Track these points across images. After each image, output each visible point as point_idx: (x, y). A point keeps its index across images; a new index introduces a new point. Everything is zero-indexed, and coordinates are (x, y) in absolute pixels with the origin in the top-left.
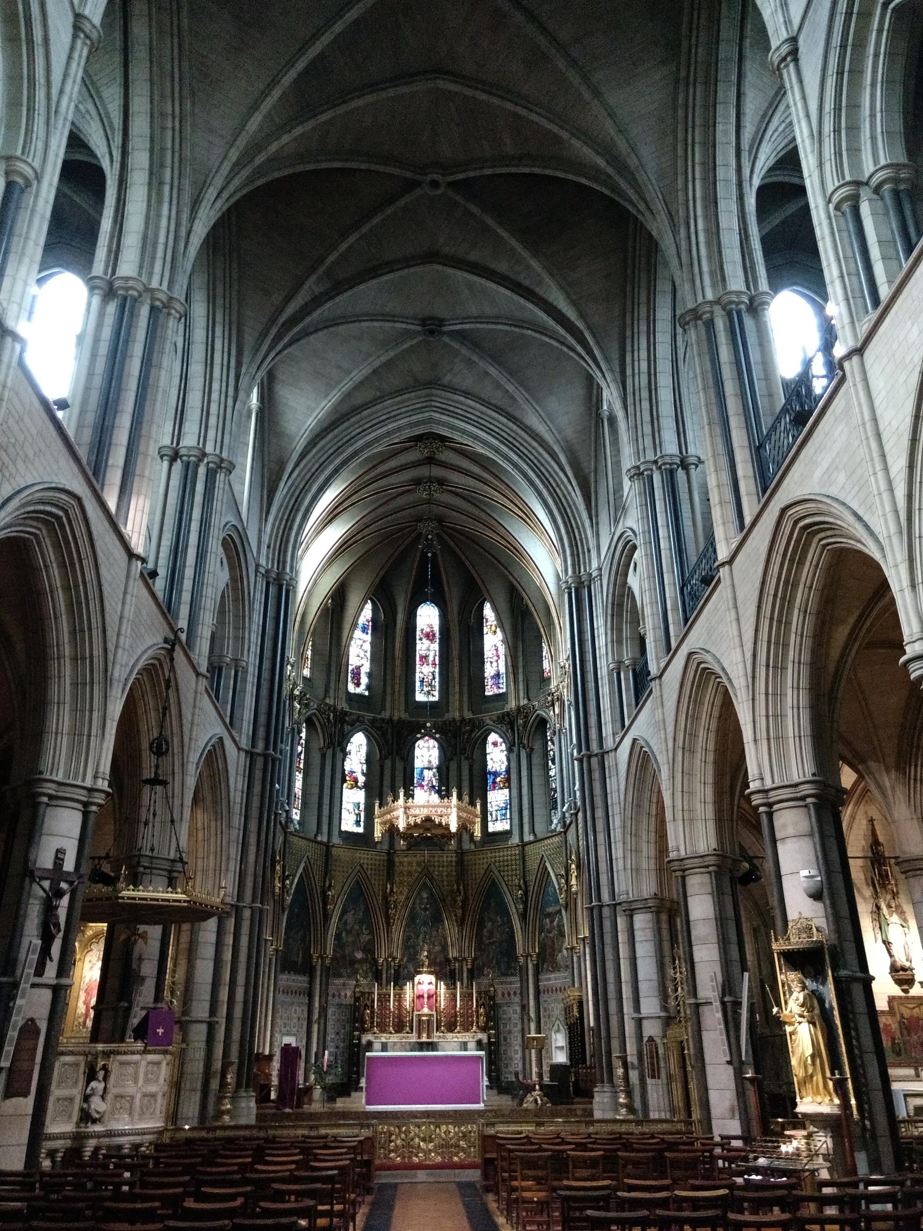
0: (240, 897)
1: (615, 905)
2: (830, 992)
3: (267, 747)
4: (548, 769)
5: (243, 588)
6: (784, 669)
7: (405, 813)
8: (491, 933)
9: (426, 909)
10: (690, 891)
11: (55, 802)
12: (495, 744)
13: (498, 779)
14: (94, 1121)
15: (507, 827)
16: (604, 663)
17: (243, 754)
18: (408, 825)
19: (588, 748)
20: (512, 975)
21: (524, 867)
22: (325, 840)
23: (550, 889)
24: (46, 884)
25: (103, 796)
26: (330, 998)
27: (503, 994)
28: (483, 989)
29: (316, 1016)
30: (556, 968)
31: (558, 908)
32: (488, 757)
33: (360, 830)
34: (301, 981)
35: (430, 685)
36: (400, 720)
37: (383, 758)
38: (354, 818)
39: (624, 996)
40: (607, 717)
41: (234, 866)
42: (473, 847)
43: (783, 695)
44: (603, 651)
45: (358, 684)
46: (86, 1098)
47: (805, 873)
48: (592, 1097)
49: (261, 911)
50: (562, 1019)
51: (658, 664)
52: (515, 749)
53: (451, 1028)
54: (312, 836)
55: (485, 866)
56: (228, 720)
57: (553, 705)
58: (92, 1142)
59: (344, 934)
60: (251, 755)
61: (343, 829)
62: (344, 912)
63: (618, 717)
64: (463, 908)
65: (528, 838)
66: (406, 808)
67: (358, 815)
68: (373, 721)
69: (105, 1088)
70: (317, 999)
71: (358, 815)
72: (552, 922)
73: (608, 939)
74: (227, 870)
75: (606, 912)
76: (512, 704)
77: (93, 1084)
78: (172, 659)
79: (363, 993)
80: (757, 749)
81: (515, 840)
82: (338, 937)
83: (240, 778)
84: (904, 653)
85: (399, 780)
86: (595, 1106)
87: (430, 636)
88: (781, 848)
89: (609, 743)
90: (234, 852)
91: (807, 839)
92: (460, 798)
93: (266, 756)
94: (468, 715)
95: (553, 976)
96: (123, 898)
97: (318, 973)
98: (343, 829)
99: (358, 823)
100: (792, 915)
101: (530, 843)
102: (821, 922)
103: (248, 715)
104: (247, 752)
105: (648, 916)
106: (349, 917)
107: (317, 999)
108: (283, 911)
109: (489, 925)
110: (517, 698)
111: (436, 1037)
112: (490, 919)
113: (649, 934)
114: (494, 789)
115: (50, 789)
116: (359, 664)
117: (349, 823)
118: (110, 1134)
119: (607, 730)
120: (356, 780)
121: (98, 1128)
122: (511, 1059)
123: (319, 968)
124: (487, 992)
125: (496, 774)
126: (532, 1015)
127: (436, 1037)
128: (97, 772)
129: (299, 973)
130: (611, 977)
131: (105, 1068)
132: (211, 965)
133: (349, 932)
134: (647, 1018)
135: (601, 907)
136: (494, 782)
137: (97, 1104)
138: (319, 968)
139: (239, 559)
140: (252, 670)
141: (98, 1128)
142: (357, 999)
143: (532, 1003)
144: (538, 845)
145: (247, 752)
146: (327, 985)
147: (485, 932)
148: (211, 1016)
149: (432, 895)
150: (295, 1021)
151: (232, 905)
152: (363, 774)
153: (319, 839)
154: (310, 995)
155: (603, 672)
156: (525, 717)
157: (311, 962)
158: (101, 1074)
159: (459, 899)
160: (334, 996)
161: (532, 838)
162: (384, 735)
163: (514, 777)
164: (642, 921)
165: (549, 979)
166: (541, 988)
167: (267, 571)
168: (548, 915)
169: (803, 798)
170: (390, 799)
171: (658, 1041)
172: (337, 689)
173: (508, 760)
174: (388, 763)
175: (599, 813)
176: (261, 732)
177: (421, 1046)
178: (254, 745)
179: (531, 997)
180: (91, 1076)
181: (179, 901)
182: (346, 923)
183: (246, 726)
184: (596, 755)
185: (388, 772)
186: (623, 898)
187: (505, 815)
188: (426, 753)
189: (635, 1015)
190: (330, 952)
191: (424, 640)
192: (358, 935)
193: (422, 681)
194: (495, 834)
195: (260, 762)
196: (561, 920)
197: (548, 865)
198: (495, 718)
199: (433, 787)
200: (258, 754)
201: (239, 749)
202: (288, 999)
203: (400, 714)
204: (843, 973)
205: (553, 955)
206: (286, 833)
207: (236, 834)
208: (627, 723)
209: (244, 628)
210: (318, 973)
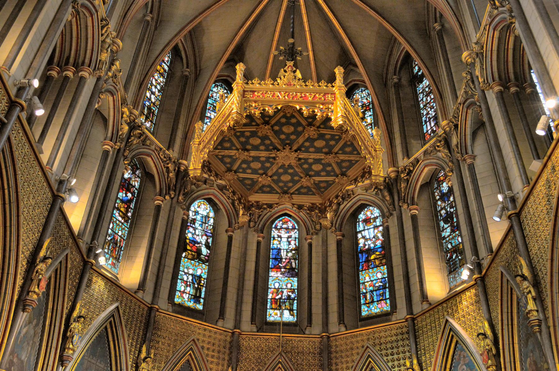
4: (440, 230)
15: (386, 307)
32: (359, 236)
33: (200, 307)
38: (192, 292)
42: (343, 329)
55: (361, 351)
61: (177, 300)
67: (198, 290)
71: (198, 290)
98: (177, 300)
99: (196, 298)
114: (368, 268)
117: (184, 295)
120: (199, 252)
125: (370, 251)
136: (368, 261)
152: (207, 246)
161: (426, 306)
173: (386, 233)
187: (384, 293)
199: (292, 269)
206: (85, 263)
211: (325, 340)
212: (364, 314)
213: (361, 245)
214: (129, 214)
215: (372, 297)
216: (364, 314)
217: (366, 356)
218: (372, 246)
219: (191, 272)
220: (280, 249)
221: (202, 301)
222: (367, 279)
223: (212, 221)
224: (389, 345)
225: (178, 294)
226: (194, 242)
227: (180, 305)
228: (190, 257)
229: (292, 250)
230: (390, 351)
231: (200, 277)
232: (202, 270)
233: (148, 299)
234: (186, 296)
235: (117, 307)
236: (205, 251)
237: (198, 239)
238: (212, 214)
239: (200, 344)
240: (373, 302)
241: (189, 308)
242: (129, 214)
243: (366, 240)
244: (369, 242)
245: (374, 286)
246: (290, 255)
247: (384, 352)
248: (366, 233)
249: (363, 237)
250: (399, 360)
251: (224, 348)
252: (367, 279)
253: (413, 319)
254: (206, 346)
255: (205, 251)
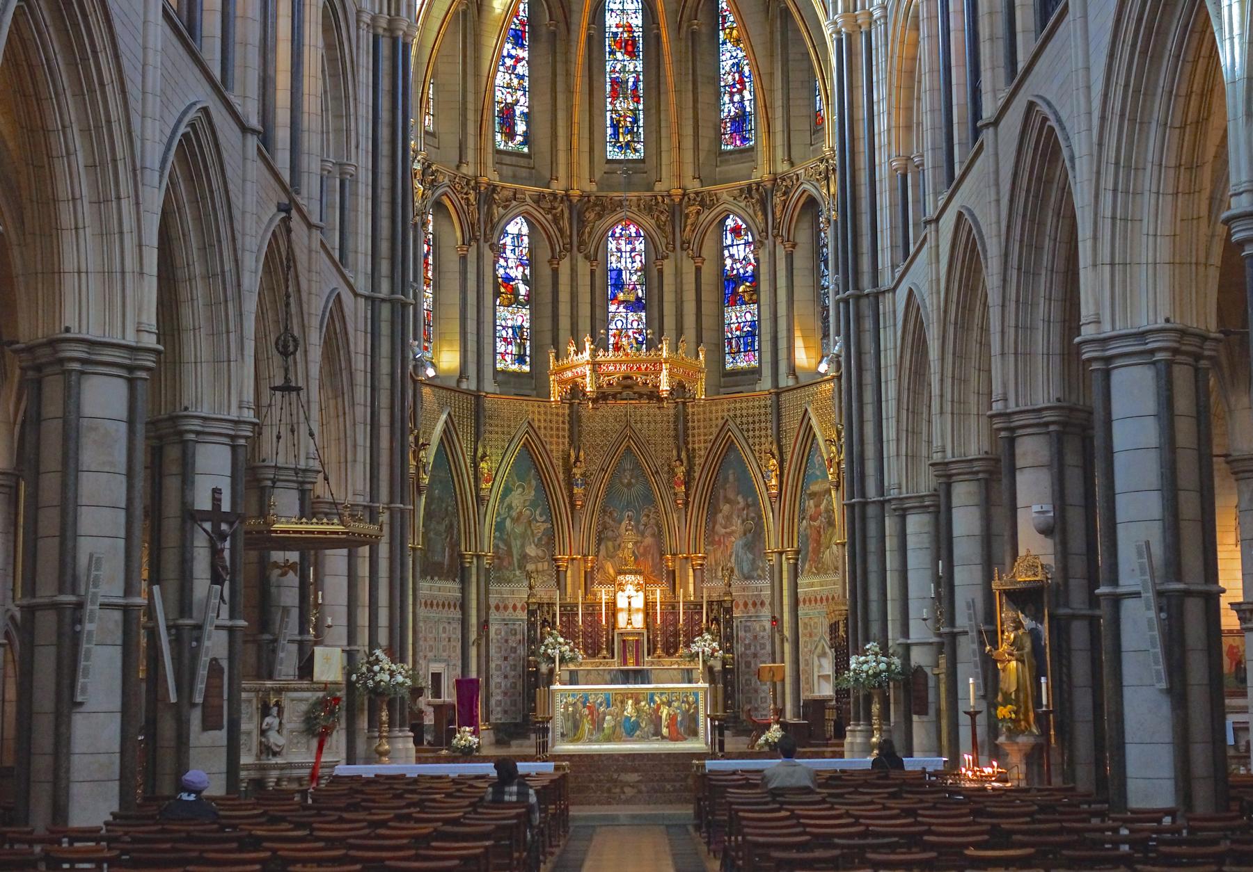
0: (374, 496)
1: (882, 503)
2: (1044, 629)
3: (393, 292)
5: (343, 57)
6: (1036, 274)
7: (594, 370)
8: (728, 518)
9: (629, 485)
10: (956, 501)
11: (201, 438)
12: (736, 231)
13: (741, 289)
14: (275, 754)
15: (754, 364)
16: (884, 158)
17: (361, 301)
18: (600, 387)
19: (856, 287)
20: (760, 577)
21: (778, 427)
22: (473, 387)
23: (817, 459)
24: (208, 526)
25: (249, 427)
26: (493, 610)
27: (746, 605)
28: (715, 597)
29: (473, 636)
30: (820, 570)
31: (827, 485)
33: (526, 368)
34: (450, 589)
35: (630, 132)
36: (585, 196)
37: (554, 259)
39: (889, 618)
40: (884, 241)
41: (363, 455)
43: (1034, 305)
44: (884, 139)
45: (511, 135)
46: (263, 733)
47: (1036, 508)
48: (845, 737)
49: (402, 511)
50: (828, 639)
51: (936, 201)
52: (769, 243)
53: (671, 648)
54: (453, 384)
55: (721, 422)
56: (337, 256)
57: (827, 178)
58: (274, 774)
59: (508, 522)
60: (373, 301)
61: (499, 366)
62: (507, 491)
63: (900, 242)
64: (687, 484)
65: (785, 381)
66: (595, 365)
68: (539, 199)
69: (280, 723)
70: (474, 612)
71: (521, 346)
72: (818, 506)
73: (872, 546)
74: (355, 461)
75: (871, 511)
76: (762, 173)
77: (268, 720)
78: (289, 231)
79: (540, 605)
80: (1003, 364)
81: (766, 384)
82: (500, 527)
83: (361, 335)
84: (1079, 335)
85: (584, 323)
86: (846, 747)
87: (629, 47)
88: (1020, 478)
89: (886, 281)
90: (363, 437)
91: (1045, 470)
92: (675, 348)
93: (392, 302)
94: (693, 186)
95: (816, 580)
96: (275, 532)
97: (474, 579)
100: (1022, 552)
101: (789, 390)
102: (1049, 560)
103: (362, 243)
104: (366, 298)
105: (926, 518)
106: (516, 499)
107: (474, 612)
108: (420, 493)
109: (726, 508)
110: (772, 160)
111: (647, 663)
112: (728, 501)
113: (926, 540)
114: (734, 304)
115: (195, 425)
116: (509, 100)
118: (290, 766)
119: (885, 259)
120: (515, 292)
121: (279, 760)
122: (756, 691)
123: (474, 570)
124: (720, 603)
126: (787, 633)
127: (647, 663)
128: (241, 402)
129: (447, 579)
130: (874, 594)
131: (277, 704)
132: (344, 582)
133: (516, 520)
134: (916, 644)
135: (864, 505)
137: (274, 738)
138: (474, 570)
139: (340, 35)
140: (365, 177)
141: (279, 760)
142: (531, 613)
143: (786, 616)
144: (798, 393)
145: (366, 298)
146: (487, 592)
147: (720, 517)
148: (349, 644)
149: (638, 465)
150: (445, 643)
151: (365, 507)
152: (525, 281)
153: (464, 386)
154: (464, 607)
155: (883, 173)
156: (785, 194)
157: (462, 563)
158: (275, 710)
159: (680, 471)
160: (497, 608)
162: (556, 220)
163: (764, 286)
164: (917, 524)
165: (812, 585)
166: (801, 599)
167: (374, 19)
168: (813, 495)
169: (1047, 424)
170: (572, 349)
171: (928, 670)
172: (479, 150)
174: (564, 267)
175: (869, 378)
176: (385, 267)
177: (627, 676)
178: (375, 286)
179: (786, 609)
180: (265, 711)
181: (337, 533)
182: (510, 507)
183: (362, 261)
184: (868, 295)
185: (564, 278)
186: (894, 493)
188: (626, 253)
189: (902, 641)
190: (487, 549)
191: (619, 56)
192: (530, 523)
193: (615, 126)
194: (735, 373)
195: (385, 311)
196: (830, 503)
197: (814, 422)
198: (736, 193)
200: (383, 300)
201: (356, 295)
202: (434, 614)
203: (584, 185)
204: (1062, 611)
205: (817, 551)
207: (362, 412)
208: (912, 250)
209: (348, 116)
210: (474, 579)
211: (681, 406)
212: (728, 367)
213: (728, 268)
214: (430, 274)
215: (738, 345)
216: (728, 367)
217: (726, 428)
218: (742, 271)
219: (510, 323)
220: (620, 270)
221: (528, 359)
222: (734, 320)
223: (526, 239)
224: (751, 419)
225: (499, 357)
226: (508, 279)
227: (503, 372)
228: (506, 302)
229: (636, 271)
230: (751, 427)
231: (521, 327)
232: (522, 317)
233: (473, 387)
234: (508, 358)
235: (449, 414)
236: (523, 289)
237: (513, 273)
238: (525, 230)
239: (536, 425)
240: (739, 351)
241: (514, 373)
242: (430, 274)
243: (735, 261)
244: (739, 265)
245: (741, 330)
246: (634, 278)
247: (745, 427)
248: (733, 250)
249: (731, 256)
250: (760, 437)
251: (563, 423)
252: (734, 320)
253: (778, 394)
254: (542, 425)
255: (523, 289)
